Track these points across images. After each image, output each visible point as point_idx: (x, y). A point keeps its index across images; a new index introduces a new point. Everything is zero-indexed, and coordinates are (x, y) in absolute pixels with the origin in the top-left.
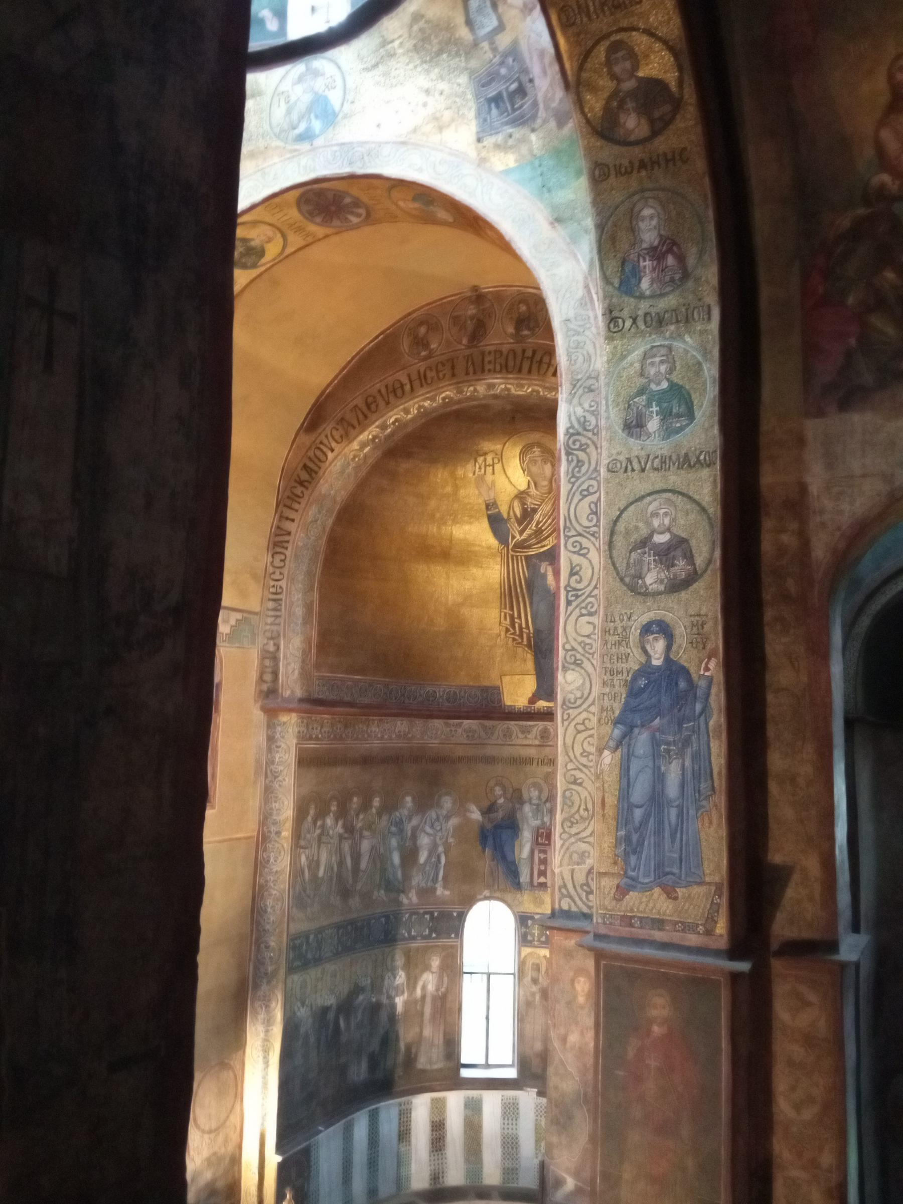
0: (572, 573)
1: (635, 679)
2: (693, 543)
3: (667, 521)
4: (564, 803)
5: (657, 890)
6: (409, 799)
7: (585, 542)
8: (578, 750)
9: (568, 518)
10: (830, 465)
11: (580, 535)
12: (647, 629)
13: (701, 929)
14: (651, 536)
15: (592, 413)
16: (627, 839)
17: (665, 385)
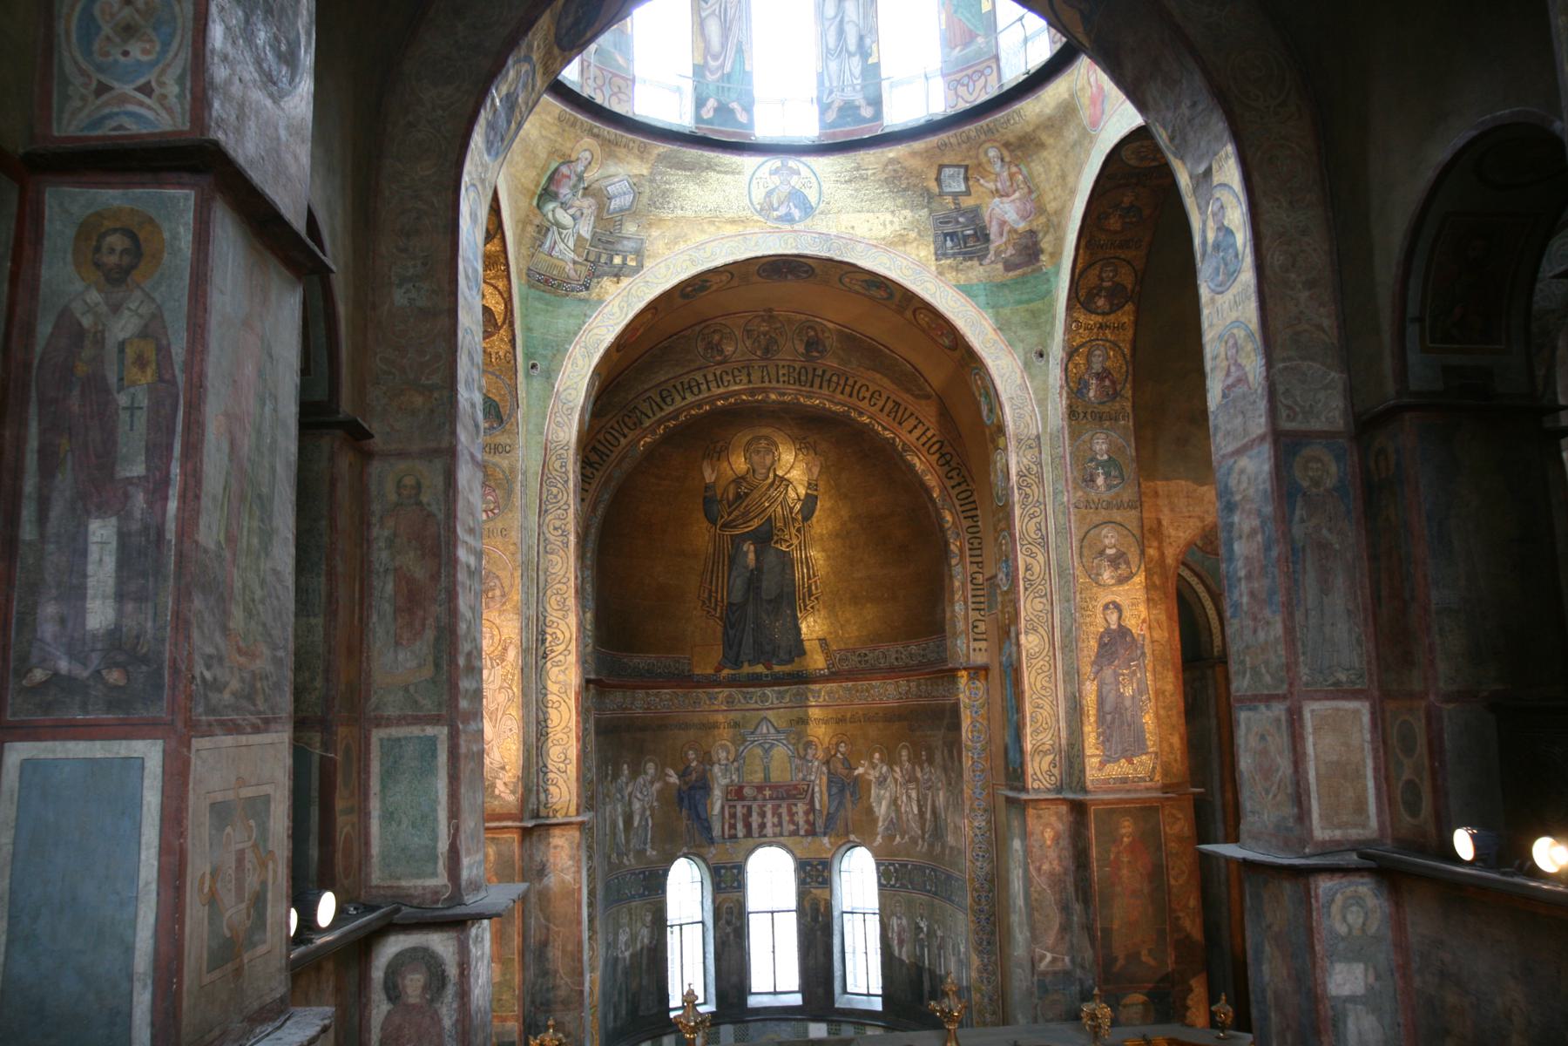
0: (1027, 569)
1: (1101, 637)
2: (1130, 556)
3: (1113, 541)
4: (1032, 721)
5: (1123, 761)
6: (625, 766)
7: (1034, 549)
8: (1039, 686)
9: (1021, 532)
10: (1172, 510)
11: (1030, 543)
12: (1106, 607)
13: (1148, 779)
14: (1104, 550)
15: (1034, 463)
16: (1103, 733)
17: (1106, 457)
